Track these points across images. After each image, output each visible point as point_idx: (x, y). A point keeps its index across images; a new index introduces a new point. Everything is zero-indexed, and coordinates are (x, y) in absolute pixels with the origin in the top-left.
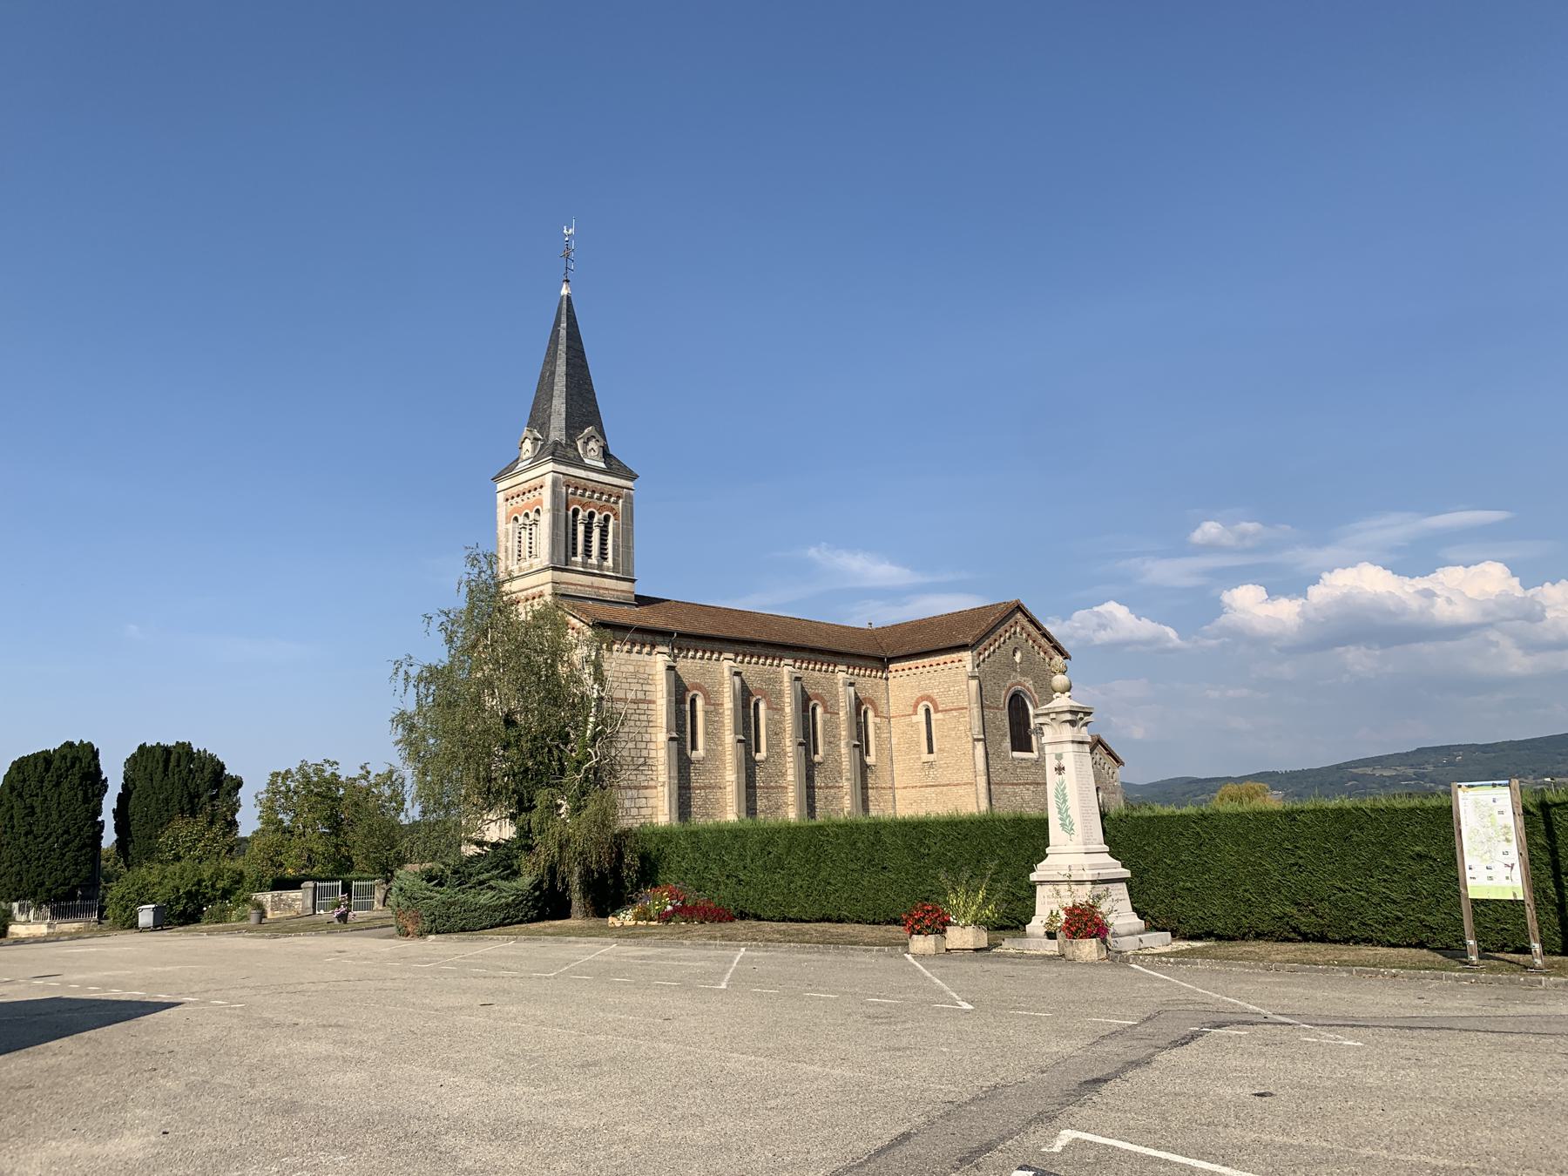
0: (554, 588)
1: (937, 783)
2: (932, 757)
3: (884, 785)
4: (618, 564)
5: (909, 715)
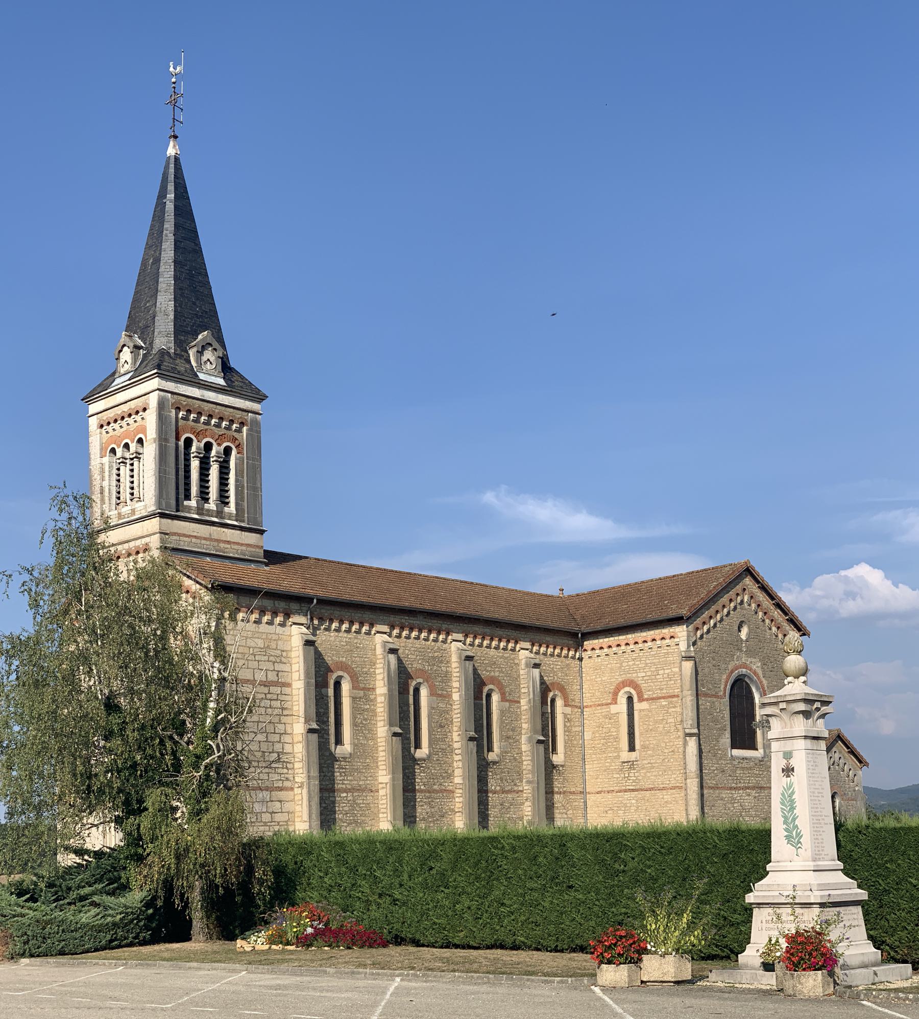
0: (162, 540)
1: (638, 787)
2: (633, 756)
3: (573, 790)
5: (607, 704)
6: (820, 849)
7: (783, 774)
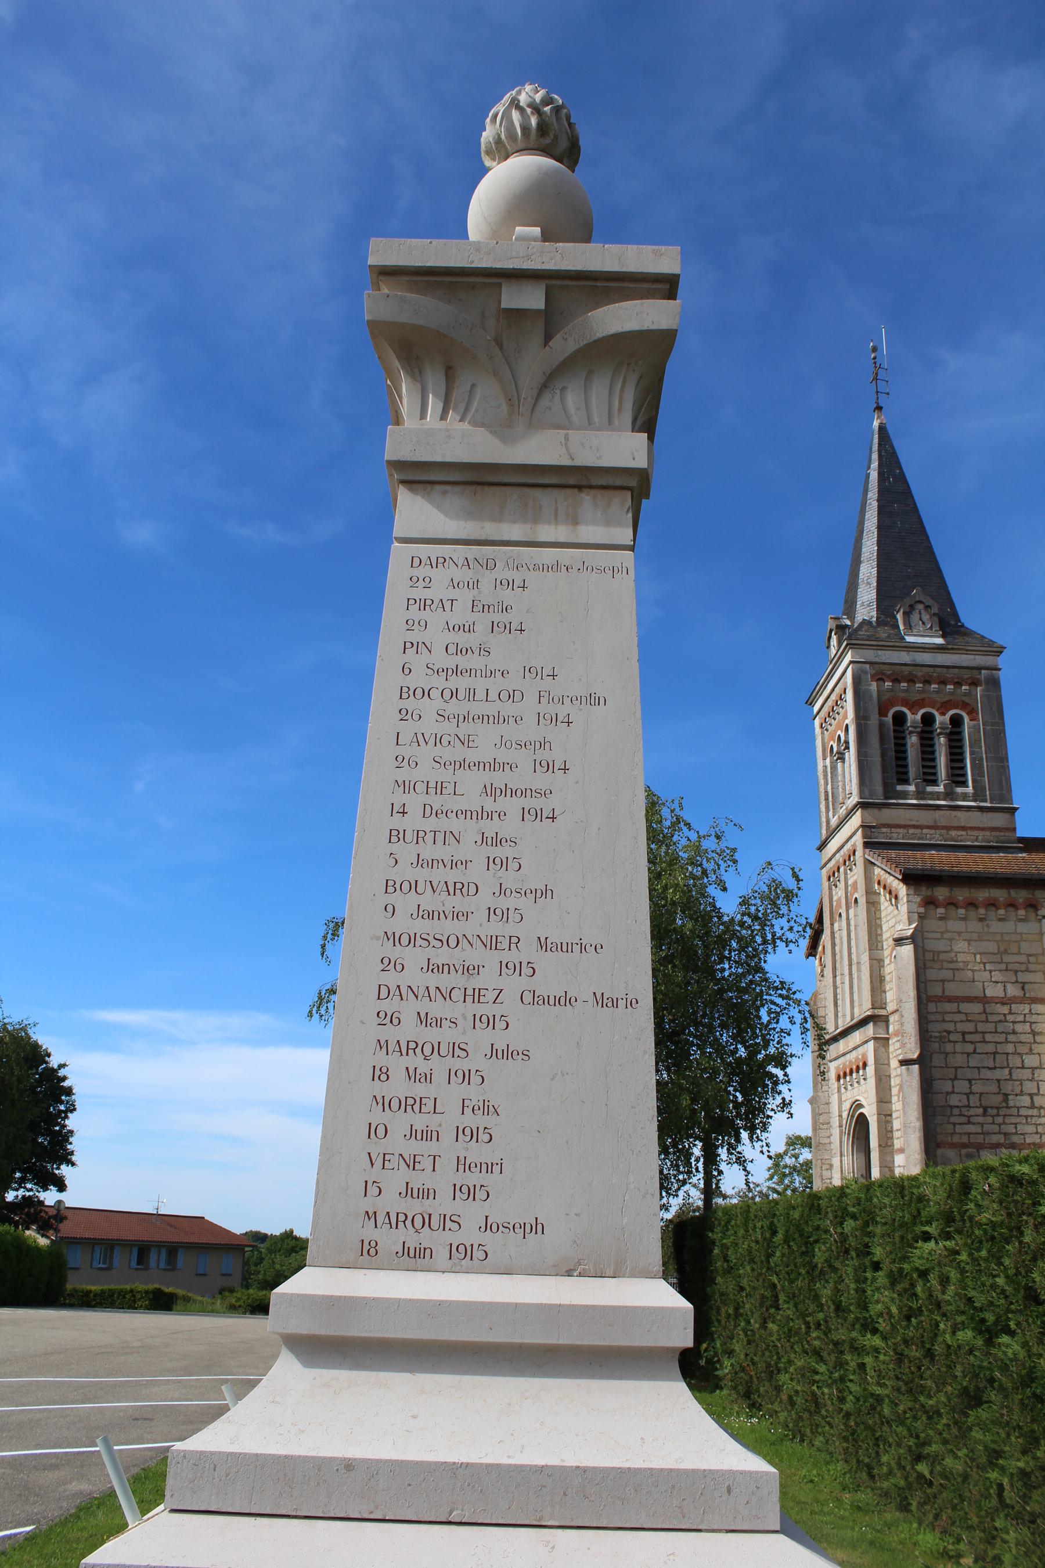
0: (864, 836)
4: (984, 788)
6: (443, 1179)
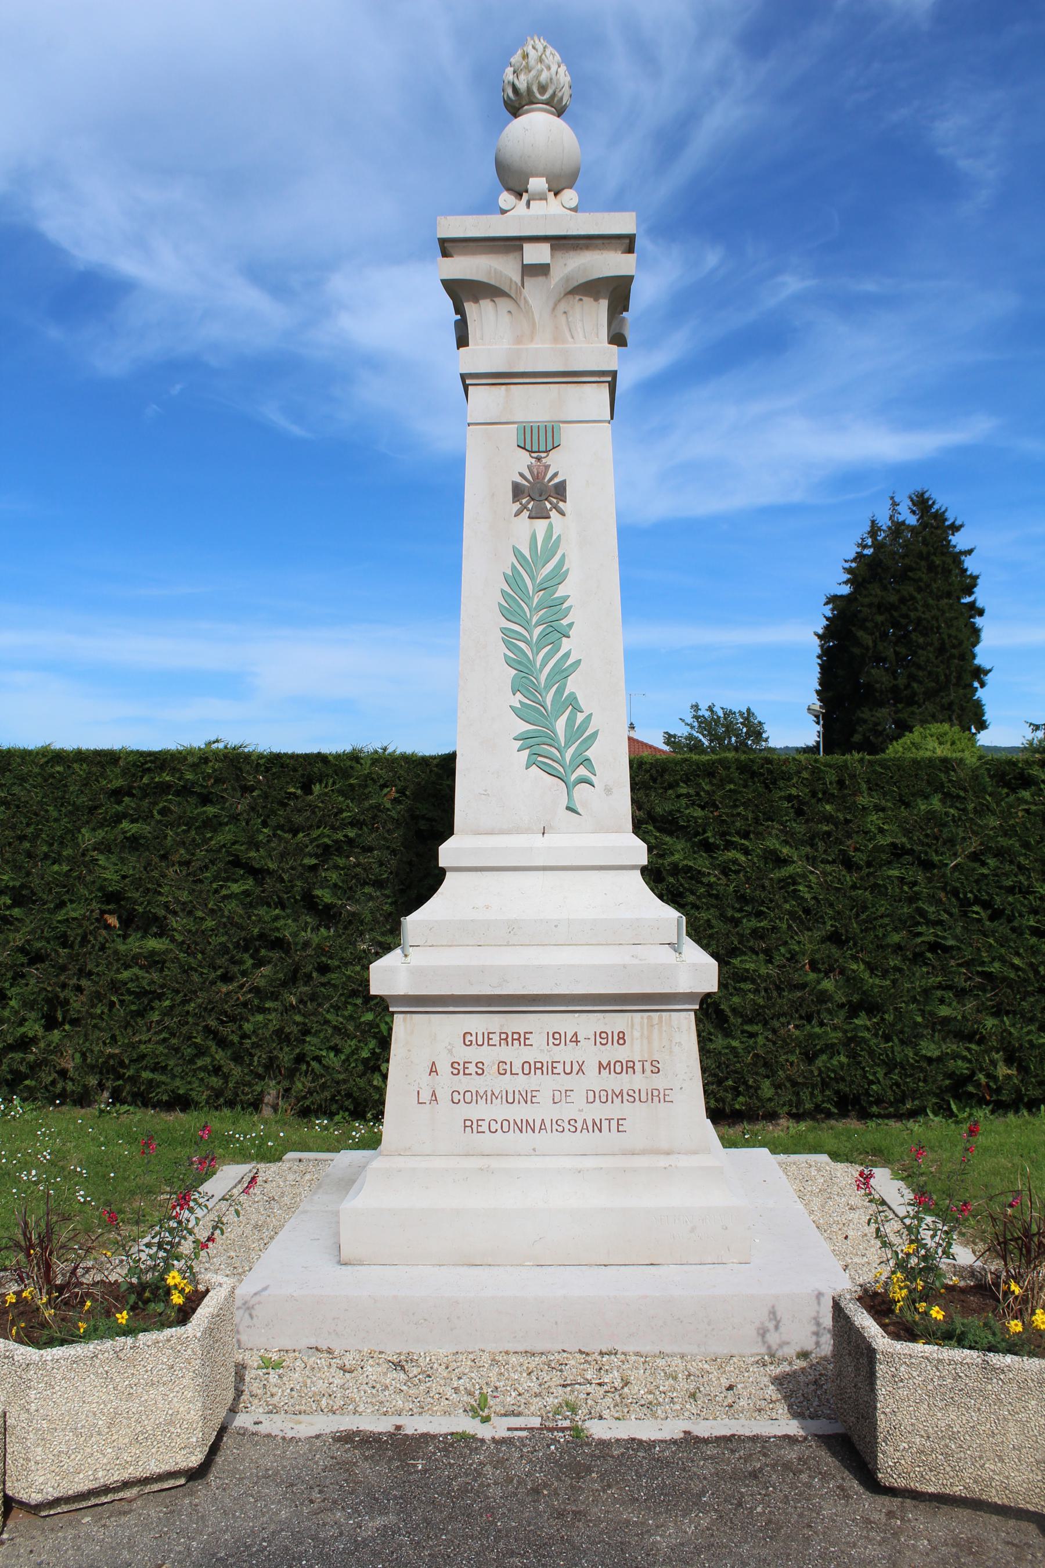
7: (517, 506)
